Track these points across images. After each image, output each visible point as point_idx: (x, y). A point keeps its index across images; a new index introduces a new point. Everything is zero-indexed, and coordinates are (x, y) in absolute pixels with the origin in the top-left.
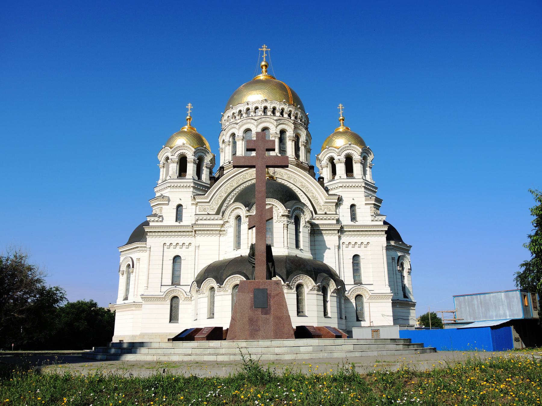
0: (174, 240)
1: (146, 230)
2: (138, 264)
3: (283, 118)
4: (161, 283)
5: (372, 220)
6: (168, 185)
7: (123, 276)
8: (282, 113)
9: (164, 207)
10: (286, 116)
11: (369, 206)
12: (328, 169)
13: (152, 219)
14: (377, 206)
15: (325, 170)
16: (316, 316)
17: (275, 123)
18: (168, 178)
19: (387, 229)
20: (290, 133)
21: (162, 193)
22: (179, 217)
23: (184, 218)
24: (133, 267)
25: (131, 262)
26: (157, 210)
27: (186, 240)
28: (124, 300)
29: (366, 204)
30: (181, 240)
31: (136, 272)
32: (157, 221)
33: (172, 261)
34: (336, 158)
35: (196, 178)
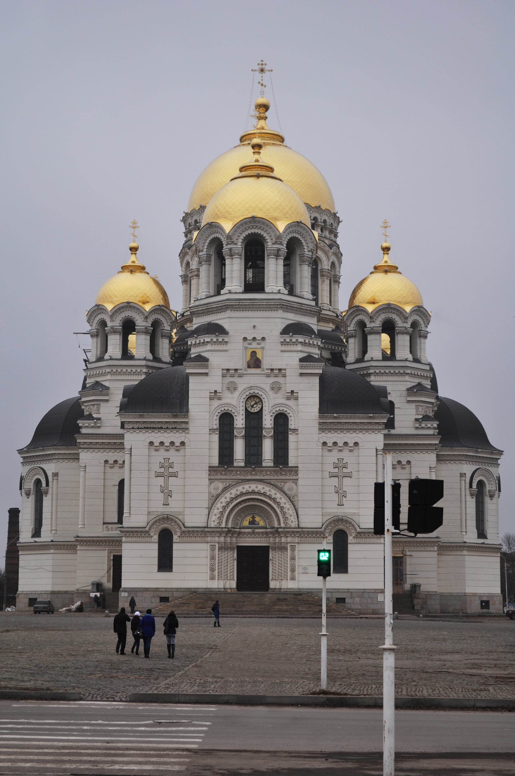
1: (78, 441)
2: (55, 481)
5: (417, 428)
6: (108, 370)
7: (28, 498)
9: (103, 404)
11: (413, 405)
12: (357, 339)
13: (86, 423)
14: (428, 404)
15: (351, 341)
18: (107, 357)
19: (438, 442)
21: (99, 379)
24: (47, 485)
25: (44, 476)
26: (91, 407)
28: (33, 536)
29: (409, 402)
31: (52, 494)
32: (93, 427)
33: (117, 487)
34: (369, 325)
35: (150, 357)
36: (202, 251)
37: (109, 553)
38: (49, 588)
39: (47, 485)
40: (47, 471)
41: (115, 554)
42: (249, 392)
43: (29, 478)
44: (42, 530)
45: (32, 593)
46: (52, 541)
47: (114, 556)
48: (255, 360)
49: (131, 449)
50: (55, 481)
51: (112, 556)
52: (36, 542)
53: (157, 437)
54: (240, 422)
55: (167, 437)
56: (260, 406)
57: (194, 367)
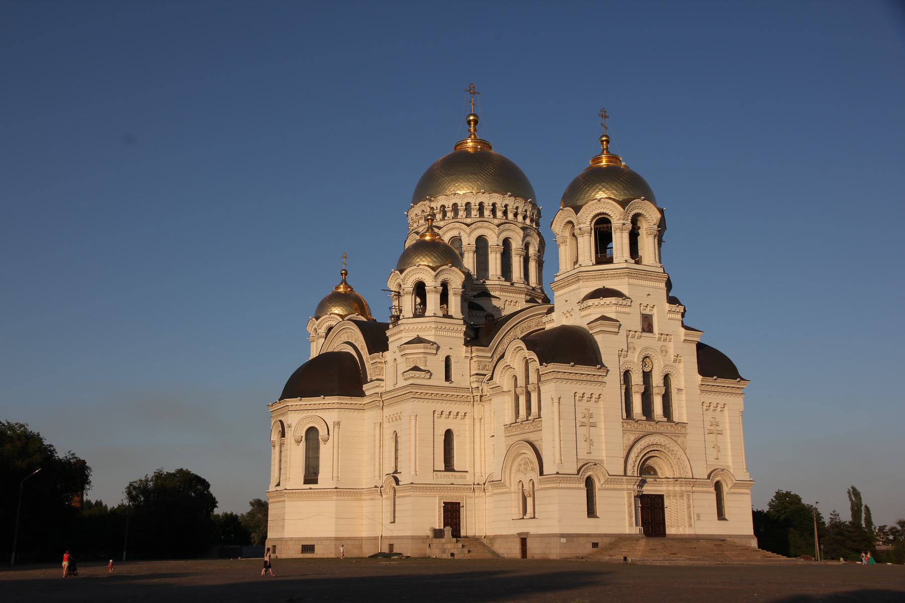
0: (446, 407)
3: (507, 221)
4: (434, 468)
8: (505, 213)
10: (511, 216)
16: (286, 508)
17: (497, 230)
20: (516, 244)
22: (448, 377)
23: (453, 377)
27: (462, 408)
30: (455, 408)
32: (422, 378)
36: (585, 223)
37: (441, 498)
38: (332, 534)
39: (328, 434)
40: (325, 420)
41: (444, 501)
42: (646, 352)
43: (300, 426)
44: (319, 477)
45: (306, 539)
46: (336, 488)
47: (444, 503)
48: (648, 325)
49: (560, 398)
50: (336, 430)
51: (442, 503)
52: (311, 489)
53: (581, 388)
54: (637, 379)
55: (588, 389)
56: (651, 366)
57: (608, 326)
